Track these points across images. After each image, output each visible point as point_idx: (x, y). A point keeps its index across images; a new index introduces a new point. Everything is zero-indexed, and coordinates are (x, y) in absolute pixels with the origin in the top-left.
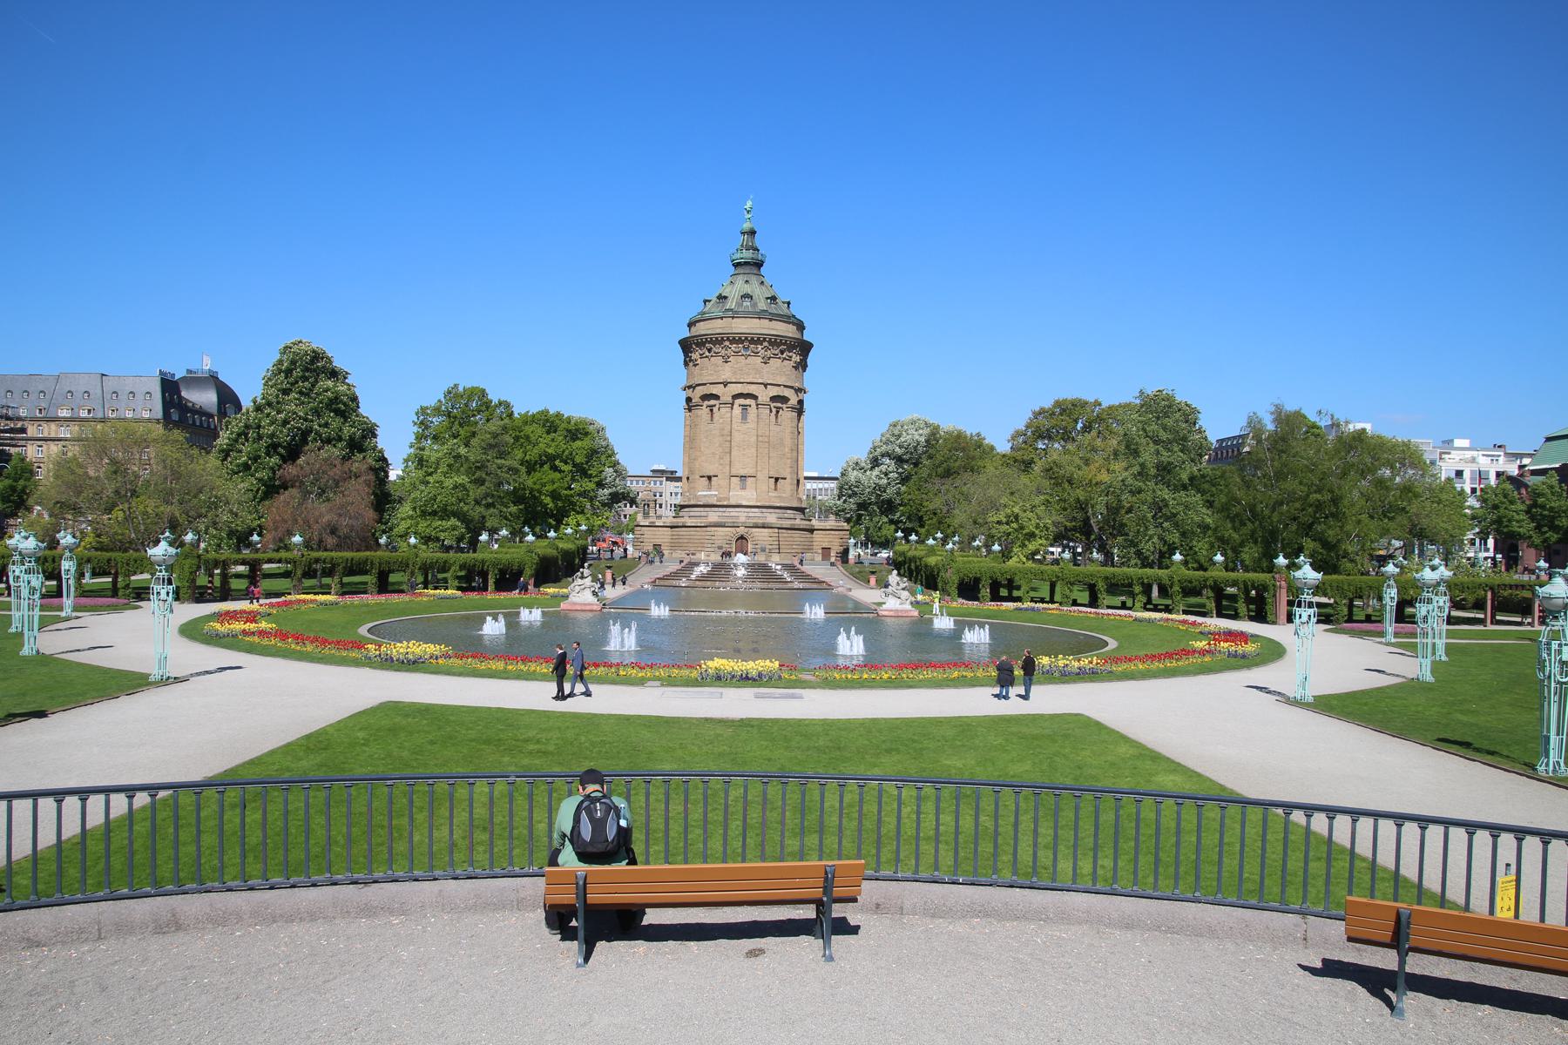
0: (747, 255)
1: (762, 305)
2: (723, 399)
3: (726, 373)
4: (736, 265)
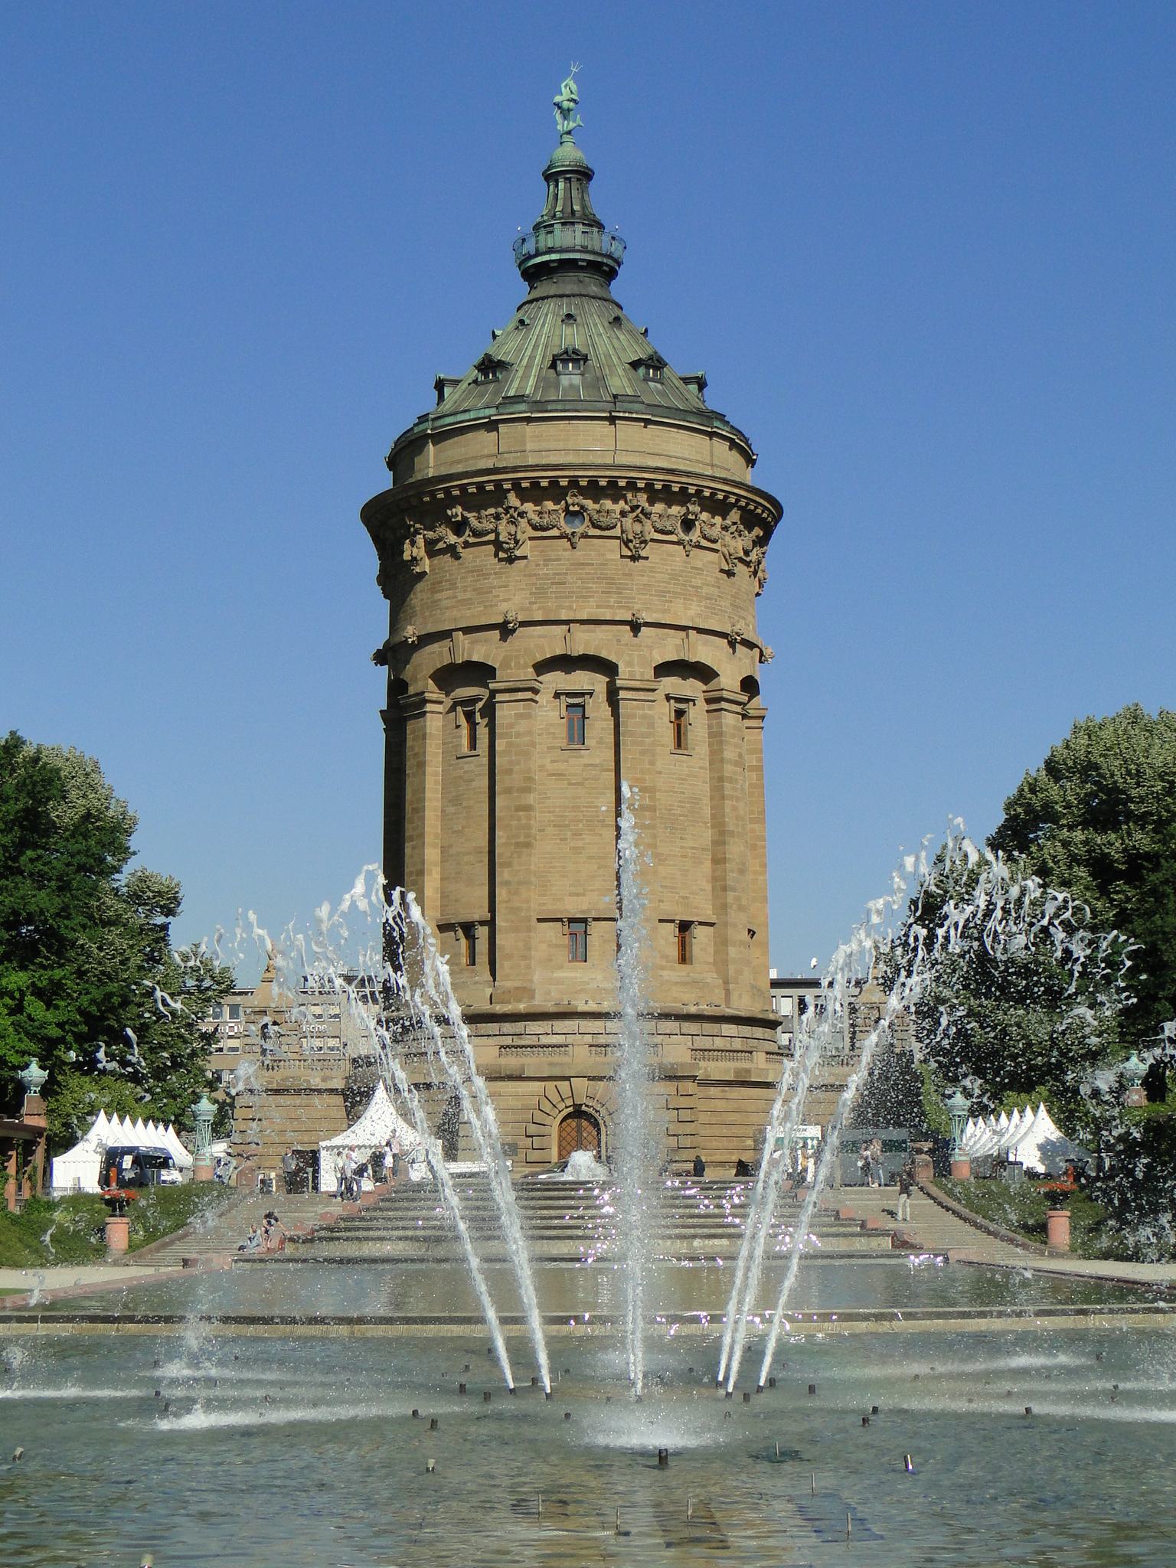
0: (570, 239)
1: (620, 382)
2: (505, 677)
3: (512, 594)
4: (534, 274)
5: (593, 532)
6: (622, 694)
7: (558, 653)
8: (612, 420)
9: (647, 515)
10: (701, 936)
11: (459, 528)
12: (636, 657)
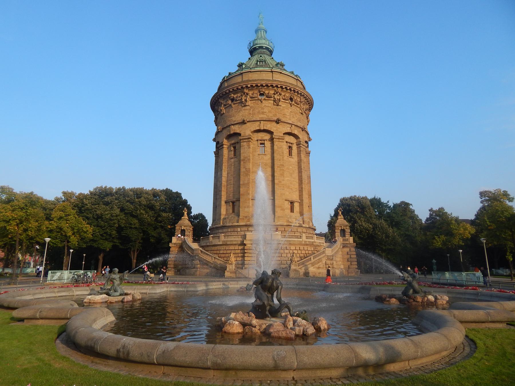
5: (266, 98)
6: (275, 140)
7: (258, 128)
8: (272, 72)
9: (280, 94)
10: (296, 205)
11: (233, 100)
12: (279, 130)
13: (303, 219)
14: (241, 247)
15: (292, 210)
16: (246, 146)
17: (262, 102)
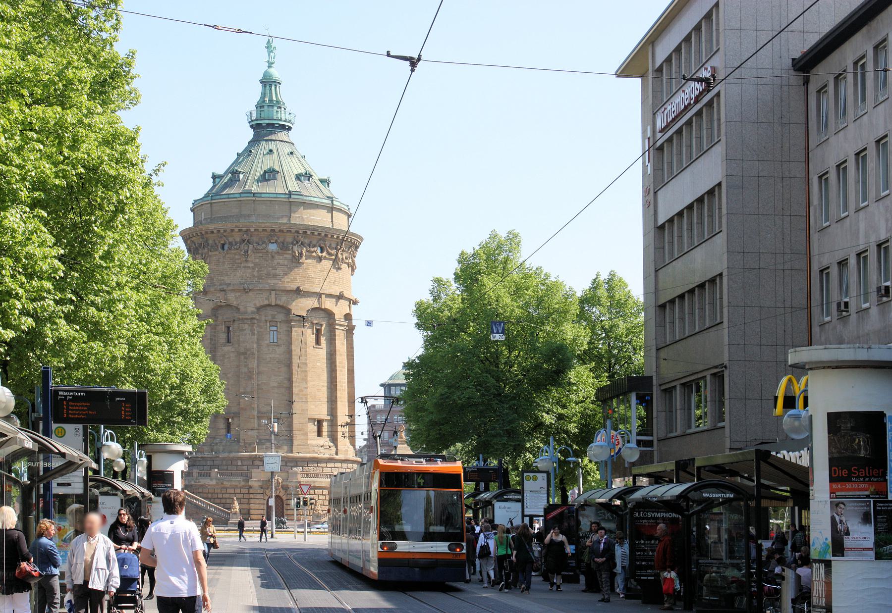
7: (266, 302)
13: (336, 447)
14: (244, 491)
15: (319, 434)
16: (248, 331)
17: (273, 257)
